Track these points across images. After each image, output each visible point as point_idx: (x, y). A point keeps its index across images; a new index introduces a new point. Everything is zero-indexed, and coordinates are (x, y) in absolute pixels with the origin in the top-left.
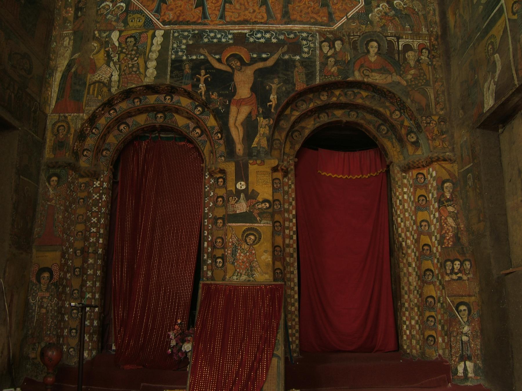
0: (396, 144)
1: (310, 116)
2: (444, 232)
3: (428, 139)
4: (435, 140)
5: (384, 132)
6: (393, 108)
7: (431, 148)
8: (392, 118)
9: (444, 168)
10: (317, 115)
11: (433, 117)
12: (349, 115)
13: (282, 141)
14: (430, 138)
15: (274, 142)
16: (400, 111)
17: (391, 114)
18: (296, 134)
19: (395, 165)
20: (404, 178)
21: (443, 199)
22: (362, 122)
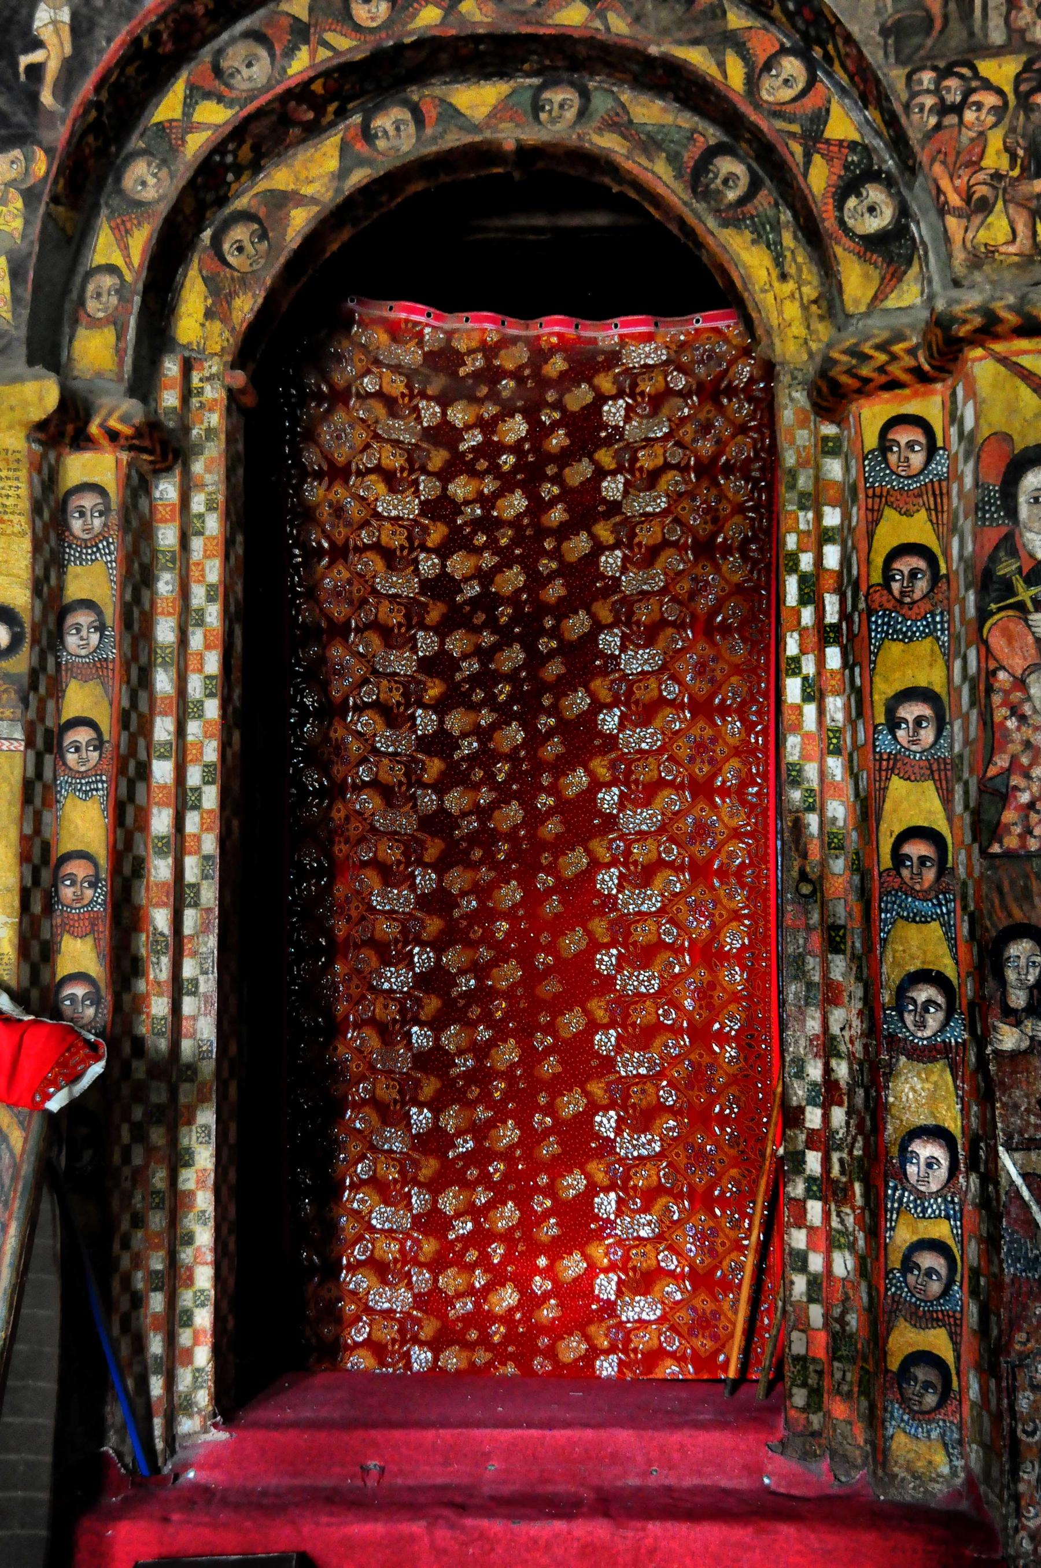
0: (798, 256)
1: (314, 130)
2: (1002, 761)
3: (942, 210)
4: (984, 207)
5: (731, 196)
6: (764, 41)
7: (959, 256)
8: (757, 104)
9: (1026, 375)
10: (357, 119)
11: (987, 68)
12: (537, 108)
13: (129, 277)
14: (955, 200)
15: (91, 288)
16: (803, 54)
17: (752, 82)
18: (240, 233)
19: (785, 379)
20: (829, 447)
21: (1006, 568)
22: (609, 143)
